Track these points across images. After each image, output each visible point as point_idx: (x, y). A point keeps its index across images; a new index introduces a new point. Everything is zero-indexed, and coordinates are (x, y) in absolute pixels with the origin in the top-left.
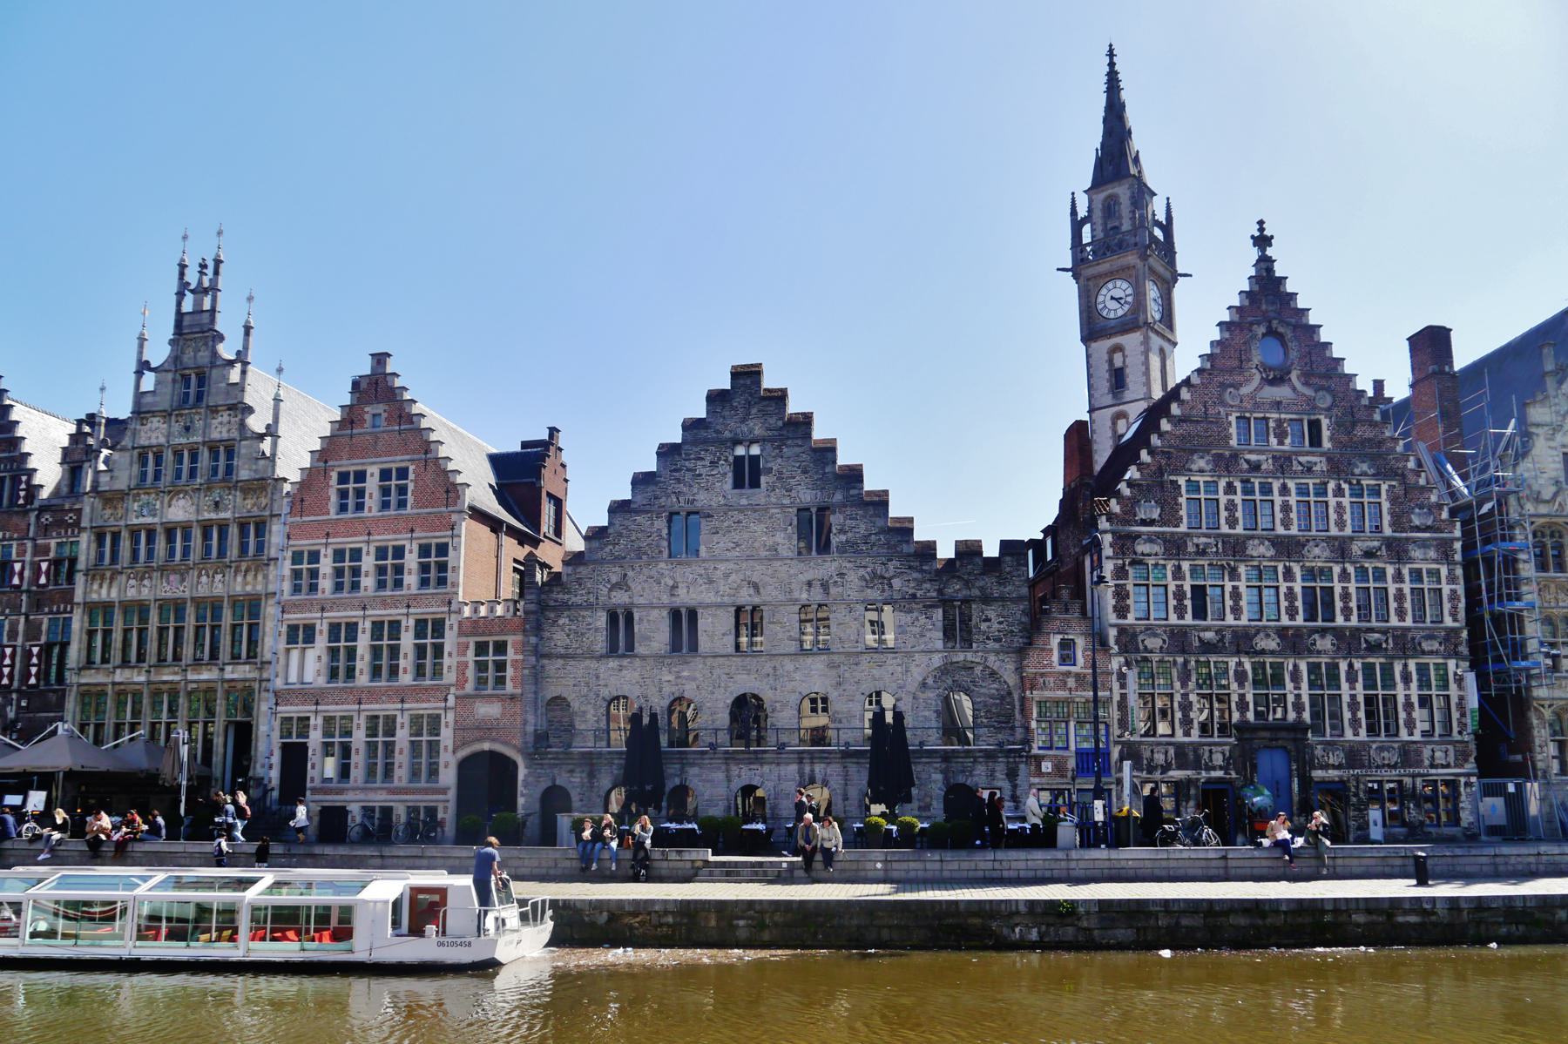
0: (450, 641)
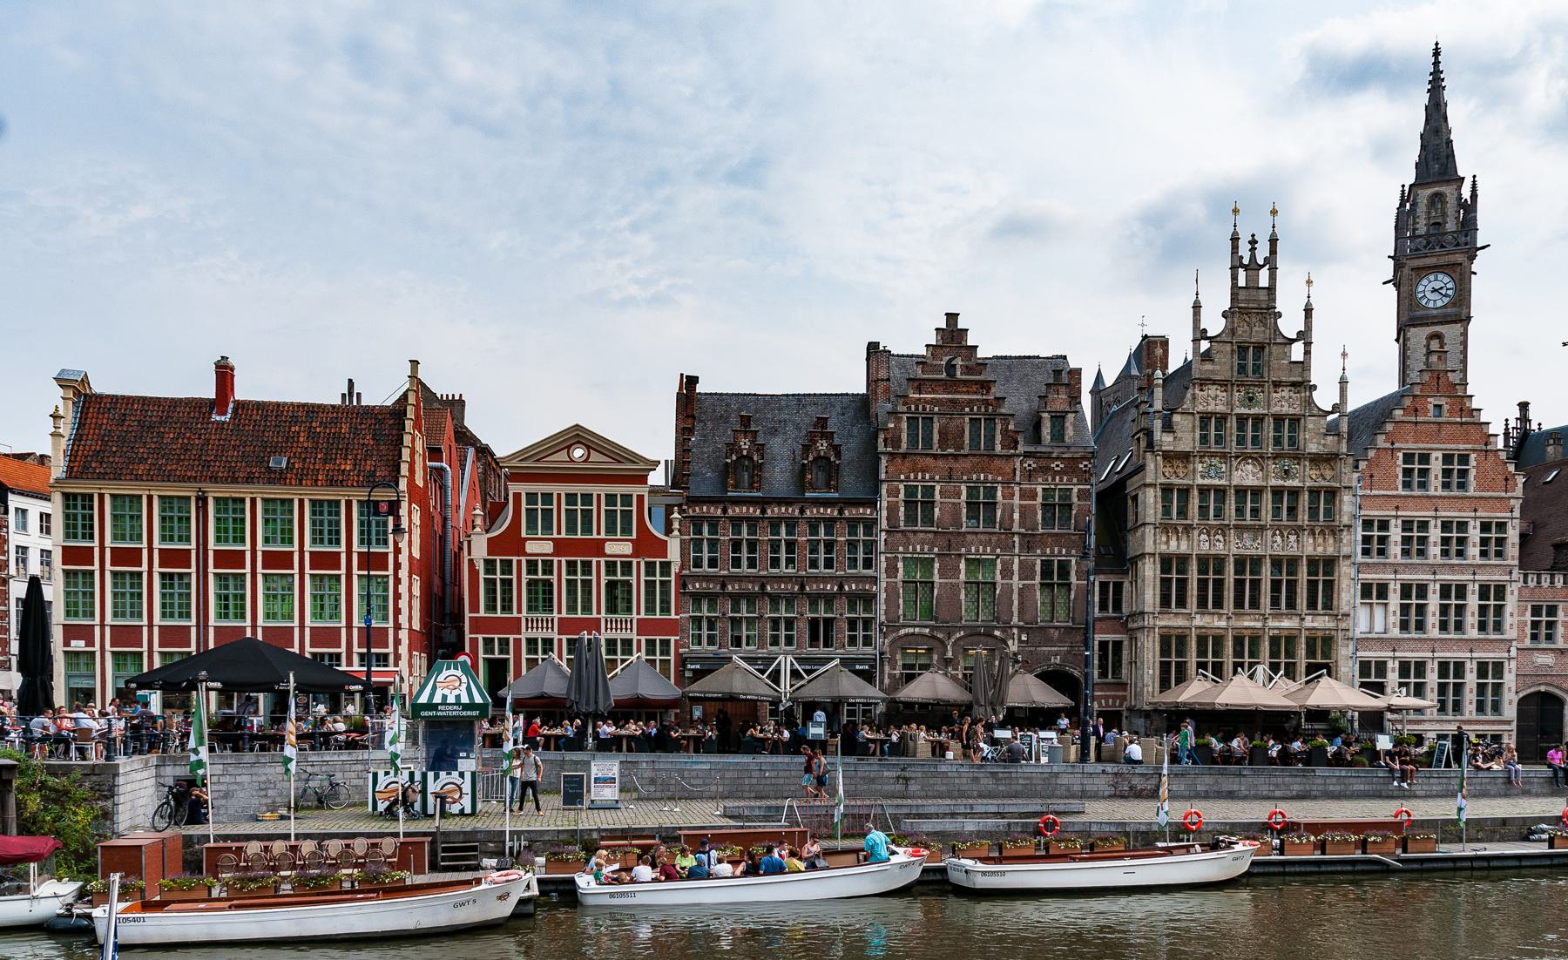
0: (1511, 603)
